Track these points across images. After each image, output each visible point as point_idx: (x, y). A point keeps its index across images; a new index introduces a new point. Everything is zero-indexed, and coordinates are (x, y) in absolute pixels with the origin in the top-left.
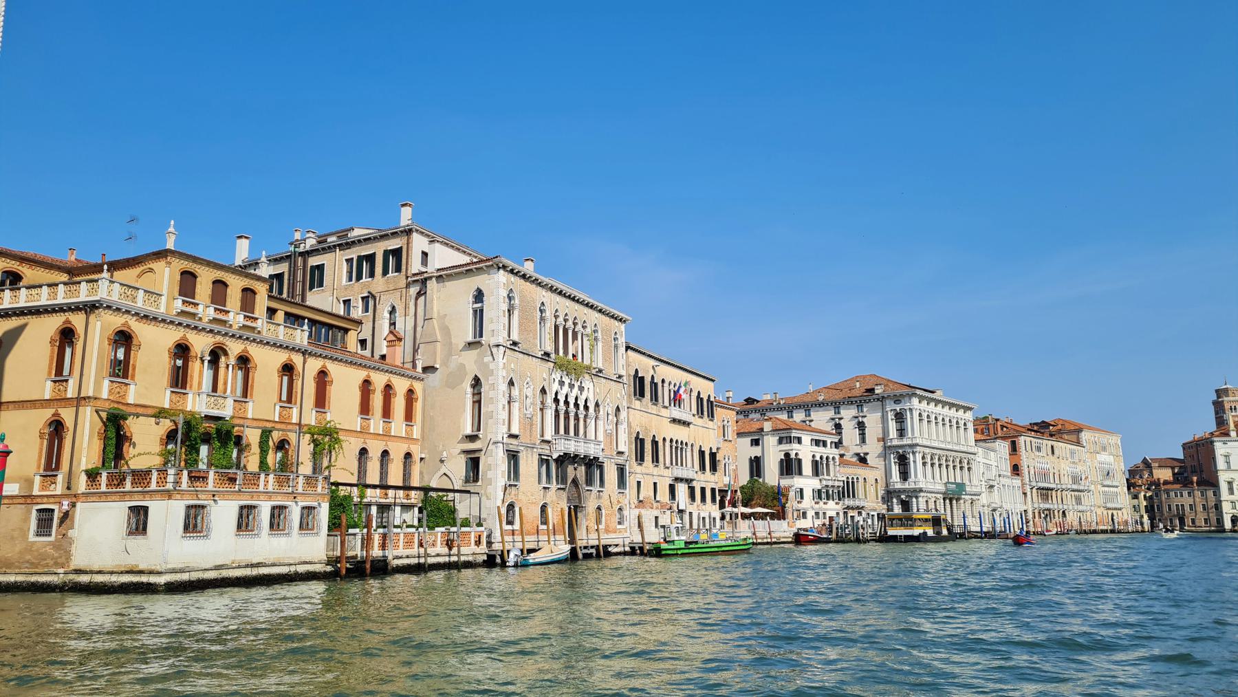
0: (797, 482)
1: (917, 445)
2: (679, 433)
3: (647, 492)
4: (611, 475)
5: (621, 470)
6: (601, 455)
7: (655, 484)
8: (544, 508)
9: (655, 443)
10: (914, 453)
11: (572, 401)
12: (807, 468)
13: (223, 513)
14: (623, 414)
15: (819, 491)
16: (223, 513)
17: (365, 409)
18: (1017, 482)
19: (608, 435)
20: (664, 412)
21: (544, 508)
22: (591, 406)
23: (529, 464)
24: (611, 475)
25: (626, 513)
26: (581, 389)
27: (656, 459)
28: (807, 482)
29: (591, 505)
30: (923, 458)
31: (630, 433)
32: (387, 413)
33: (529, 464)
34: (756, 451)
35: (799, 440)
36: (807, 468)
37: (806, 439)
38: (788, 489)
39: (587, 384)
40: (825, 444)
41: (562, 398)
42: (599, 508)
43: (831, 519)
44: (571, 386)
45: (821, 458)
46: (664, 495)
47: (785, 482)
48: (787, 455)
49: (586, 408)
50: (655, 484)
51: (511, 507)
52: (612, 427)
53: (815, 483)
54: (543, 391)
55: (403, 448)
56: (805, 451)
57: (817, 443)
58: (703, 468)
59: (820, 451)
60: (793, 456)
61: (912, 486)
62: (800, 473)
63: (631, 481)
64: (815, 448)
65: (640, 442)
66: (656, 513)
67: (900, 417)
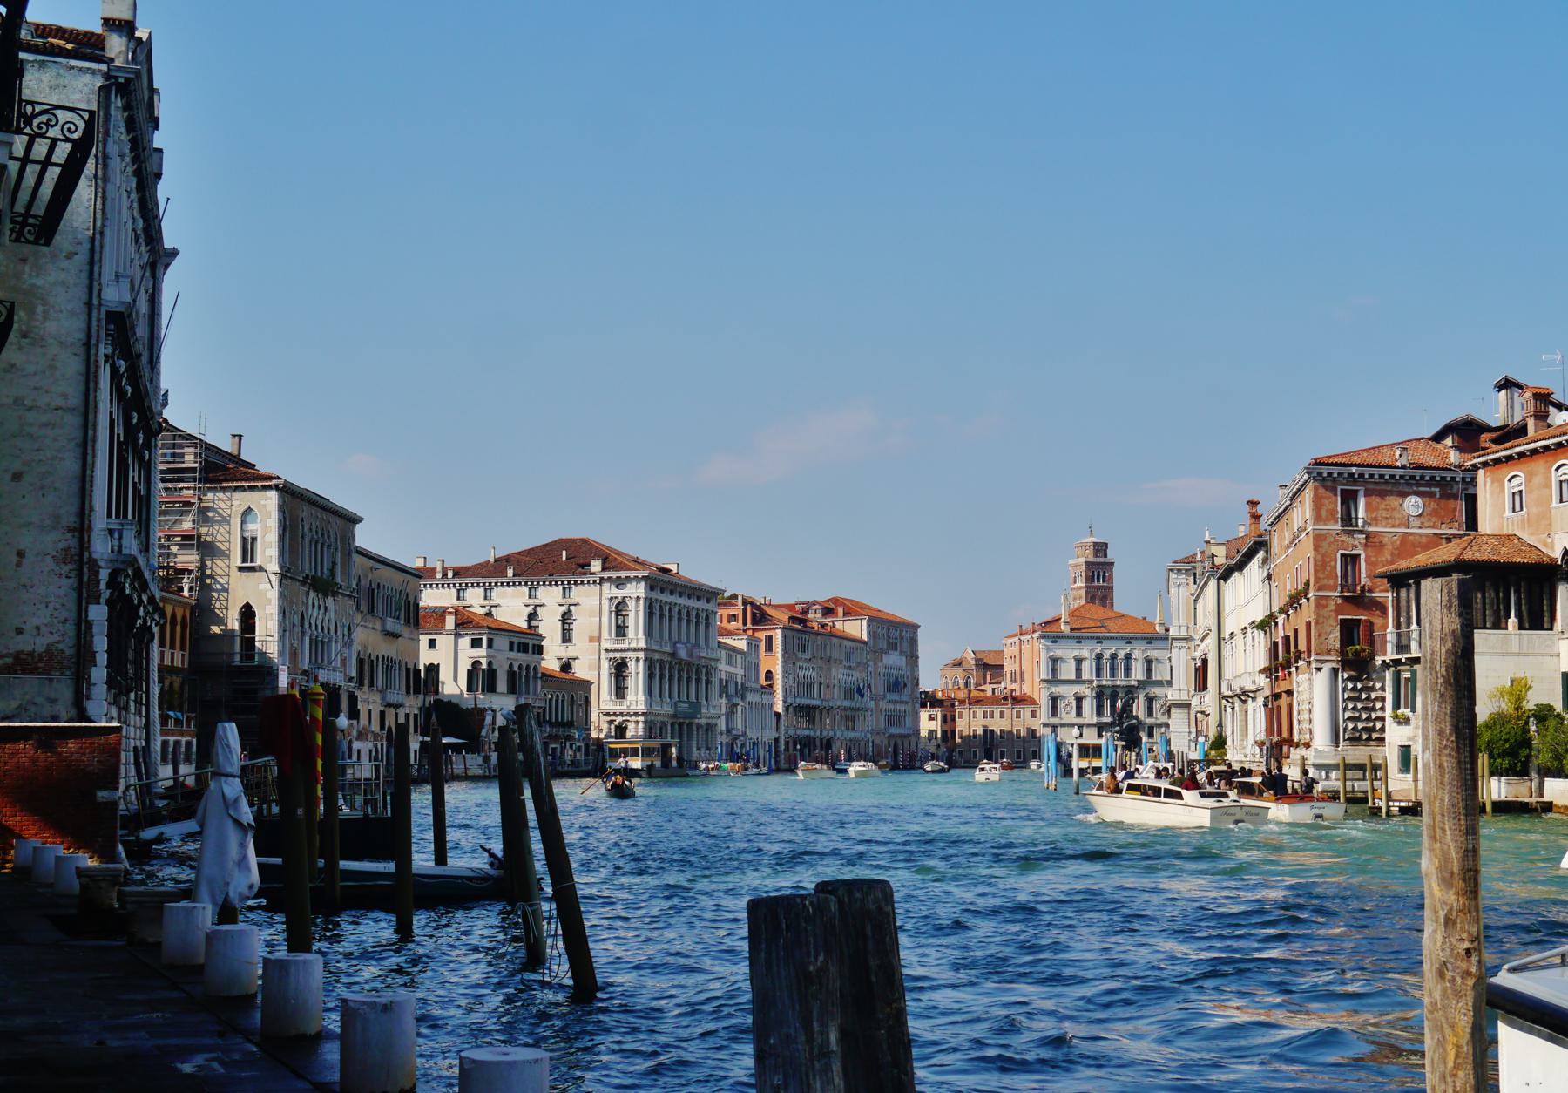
12: (502, 685)
36: (502, 685)
45: (520, 667)
64: (514, 654)
67: (620, 608)
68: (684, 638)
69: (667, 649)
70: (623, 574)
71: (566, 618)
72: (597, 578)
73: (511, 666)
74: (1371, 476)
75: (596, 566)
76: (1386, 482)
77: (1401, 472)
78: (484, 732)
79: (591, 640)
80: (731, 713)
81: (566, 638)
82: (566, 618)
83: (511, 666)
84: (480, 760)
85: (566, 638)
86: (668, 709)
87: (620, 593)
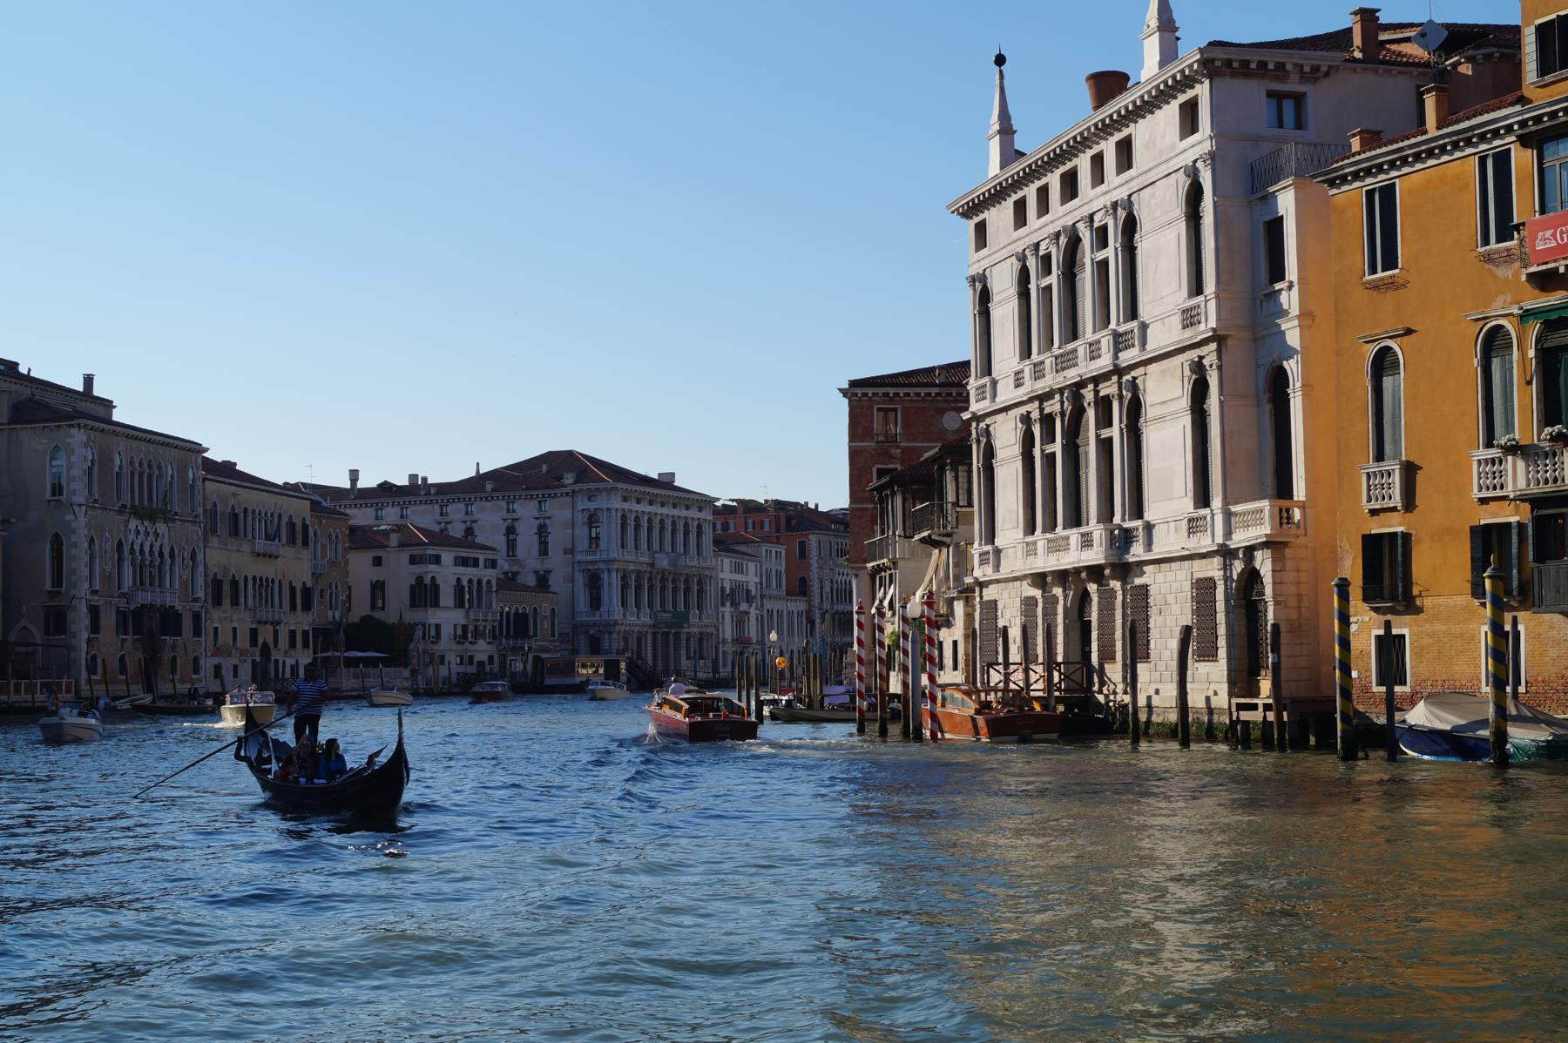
0: (433, 617)
1: (614, 560)
2: (267, 570)
3: (225, 638)
4: (187, 624)
5: (197, 617)
6: (178, 606)
7: (234, 629)
8: (122, 659)
9: (234, 583)
10: (609, 571)
12: (447, 598)
14: (200, 556)
15: (465, 628)
18: (798, 605)
19: (184, 583)
20: (246, 547)
22: (166, 552)
23: (108, 620)
24: (187, 624)
25: (202, 662)
26: (157, 535)
28: (447, 618)
29: (166, 656)
30: (624, 578)
31: (206, 575)
33: (108, 620)
34: (378, 574)
35: (437, 560)
36: (447, 598)
37: (447, 556)
38: (412, 627)
39: (162, 528)
40: (475, 563)
41: (137, 548)
42: (174, 658)
43: (481, 664)
44: (147, 534)
45: (470, 581)
46: (244, 642)
47: (412, 616)
48: (419, 579)
49: (161, 554)
50: (234, 629)
51: (94, 658)
52: (187, 574)
53: (458, 617)
54: (120, 544)
56: (447, 572)
57: (463, 562)
58: (293, 608)
59: (468, 573)
60: (428, 581)
61: (605, 617)
62: (436, 604)
63: (208, 626)
64: (462, 570)
65: (217, 584)
66: (235, 661)
68: (668, 548)
69: (646, 559)
70: (592, 486)
71: (542, 531)
72: (568, 490)
73: (459, 580)
74: (908, 394)
75: (569, 479)
76: (923, 400)
77: (937, 390)
78: (411, 646)
79: (566, 552)
80: (740, 621)
81: (544, 550)
82: (542, 531)
83: (459, 580)
84: (406, 673)
85: (544, 550)
86: (646, 619)
87: (592, 506)
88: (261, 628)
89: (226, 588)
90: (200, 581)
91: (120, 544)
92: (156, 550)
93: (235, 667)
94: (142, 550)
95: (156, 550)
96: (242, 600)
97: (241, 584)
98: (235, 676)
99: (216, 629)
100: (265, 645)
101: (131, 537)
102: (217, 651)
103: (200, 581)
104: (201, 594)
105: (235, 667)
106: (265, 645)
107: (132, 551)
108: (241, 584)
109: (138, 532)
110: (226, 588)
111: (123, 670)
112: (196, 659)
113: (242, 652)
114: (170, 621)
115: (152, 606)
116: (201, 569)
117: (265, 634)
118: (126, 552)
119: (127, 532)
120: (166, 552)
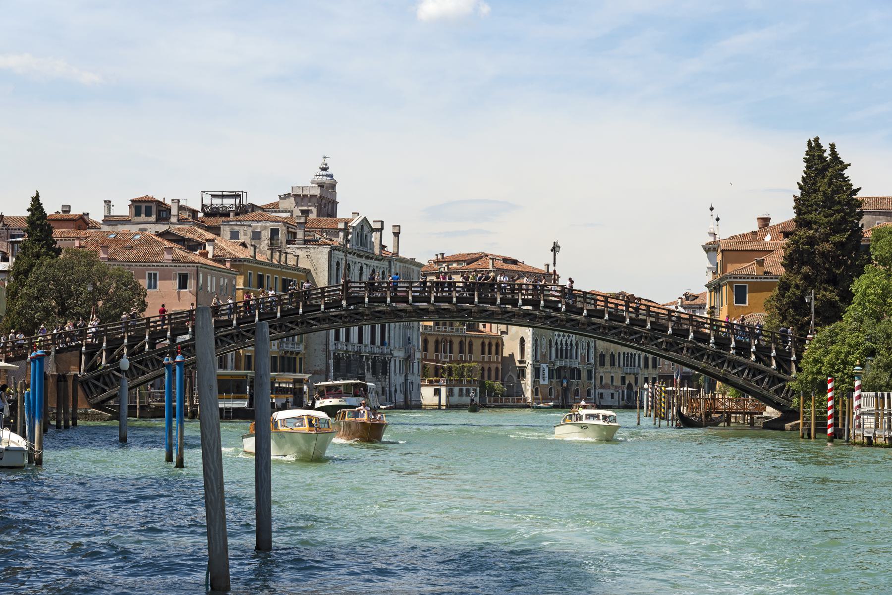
4: (584, 375)
8: (551, 389)
11: (564, 343)
13: (456, 390)
16: (456, 390)
17: (483, 352)
21: (551, 389)
22: (574, 343)
24: (584, 375)
25: (593, 391)
27: (613, 364)
32: (490, 353)
41: (559, 342)
49: (571, 345)
54: (550, 341)
55: (495, 365)
66: (612, 391)
88: (627, 377)
89: (608, 358)
90: (592, 355)
91: (550, 341)
92: (569, 343)
93: (612, 395)
94: (561, 344)
95: (569, 343)
96: (617, 363)
97: (616, 356)
98: (612, 397)
99: (602, 377)
100: (630, 385)
101: (556, 338)
102: (602, 387)
103: (592, 355)
104: (592, 361)
105: (612, 395)
106: (630, 385)
107: (557, 344)
108: (616, 356)
109: (559, 336)
110: (608, 358)
111: (550, 394)
112: (589, 391)
113: (616, 387)
114: (575, 373)
115: (565, 367)
116: (592, 350)
117: (630, 379)
118: (553, 344)
119: (554, 335)
120: (574, 343)
